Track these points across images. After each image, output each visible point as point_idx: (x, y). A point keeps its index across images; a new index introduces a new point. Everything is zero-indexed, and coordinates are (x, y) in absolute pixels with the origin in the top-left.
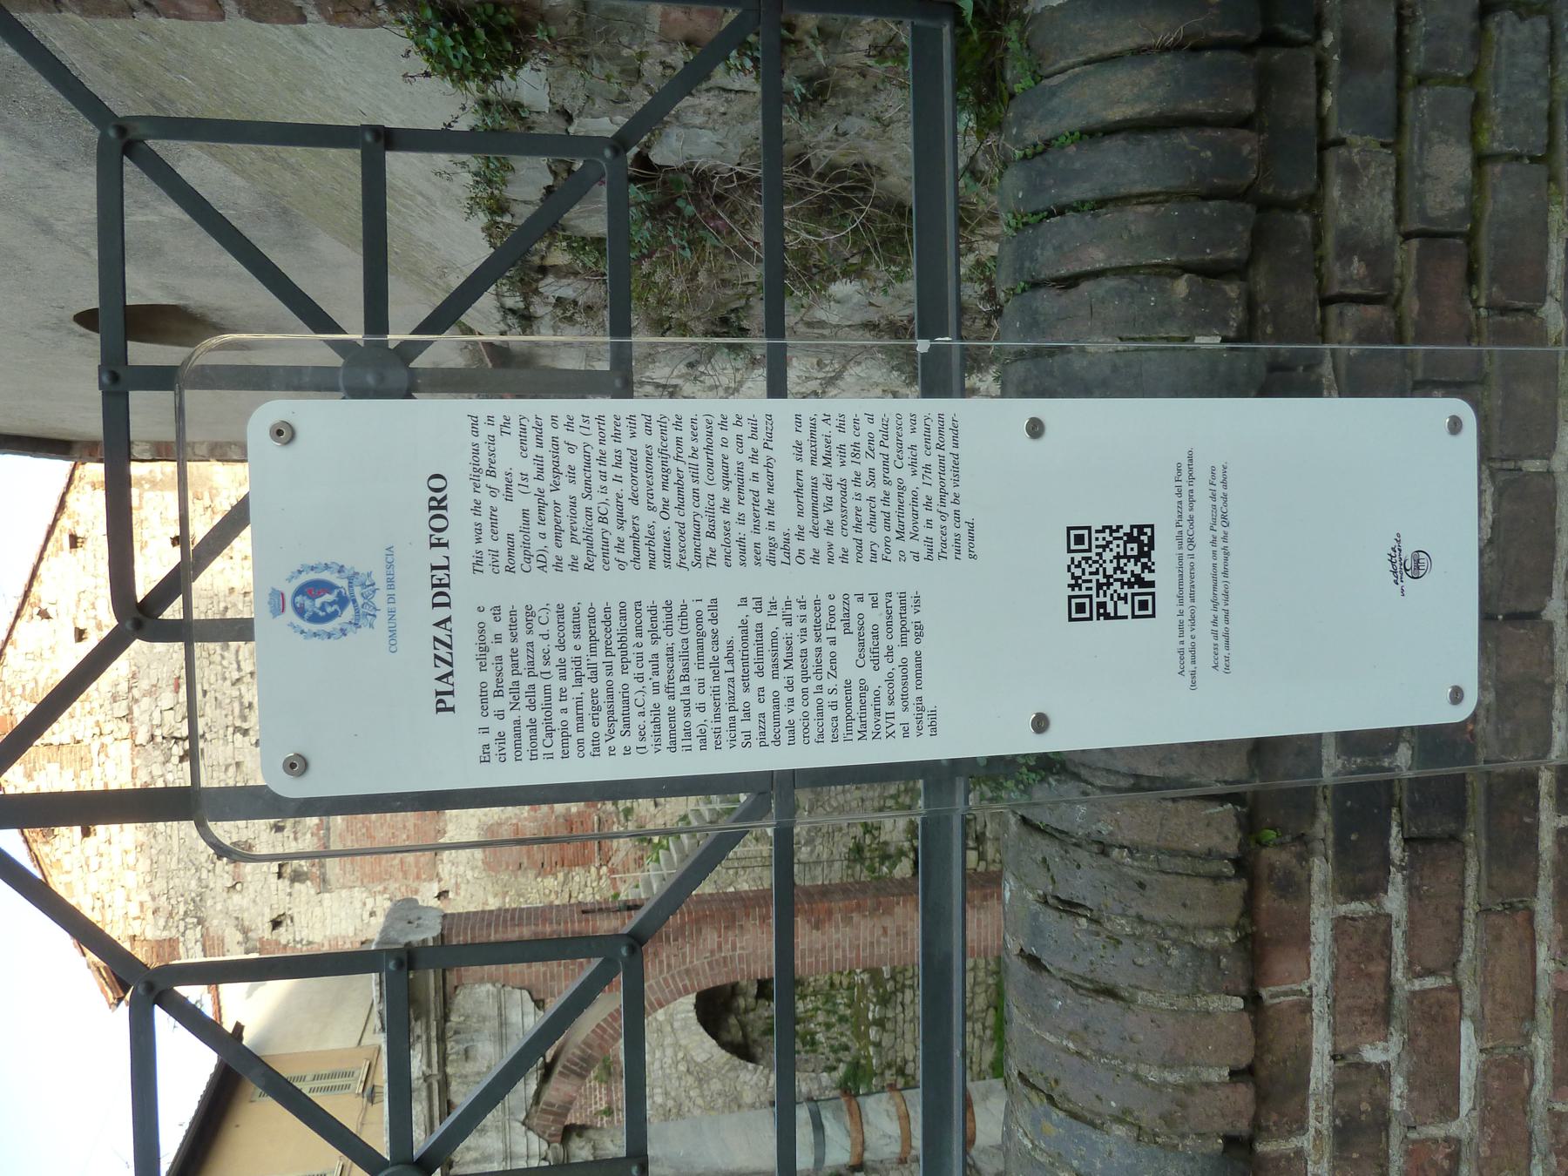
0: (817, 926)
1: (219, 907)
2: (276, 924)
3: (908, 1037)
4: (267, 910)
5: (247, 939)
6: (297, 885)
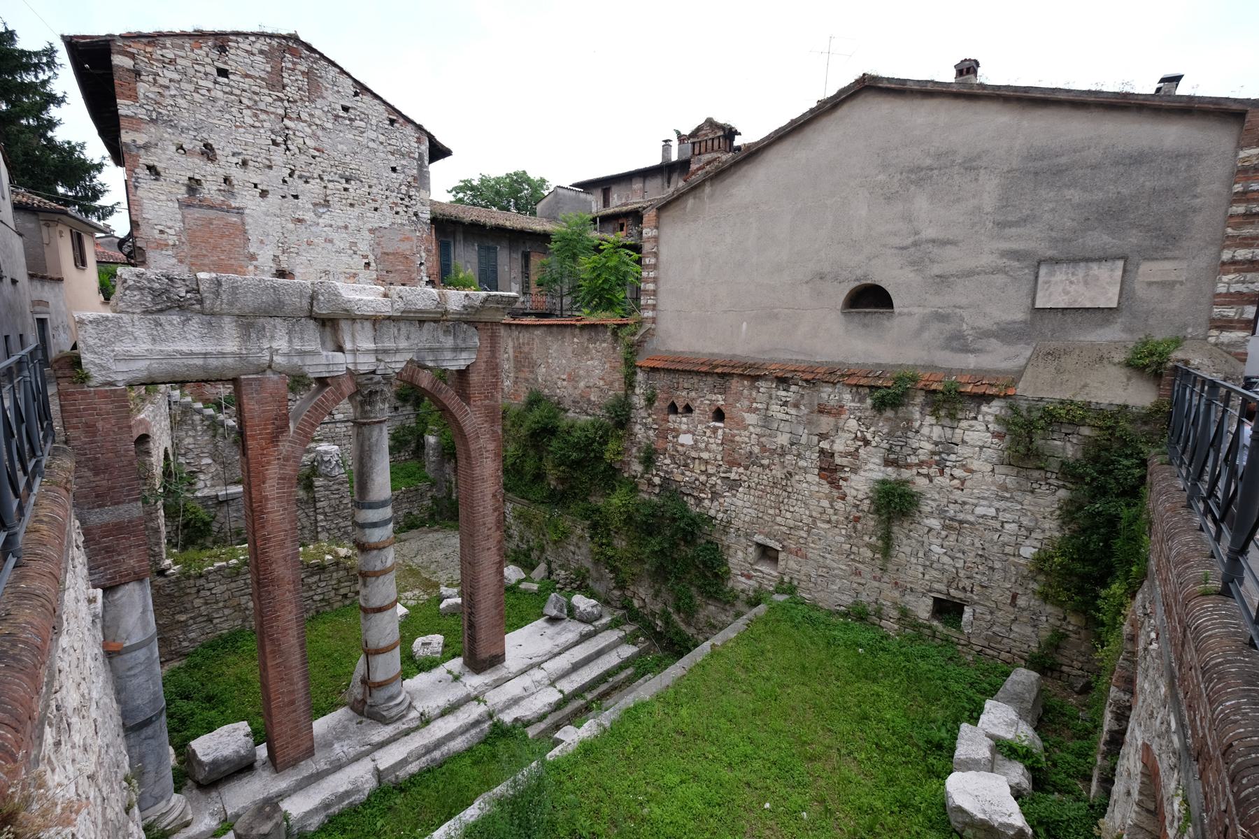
0: (494, 496)
1: (166, 136)
2: (151, 168)
3: (233, 585)
4: (164, 165)
5: (139, 148)
6: (184, 189)
